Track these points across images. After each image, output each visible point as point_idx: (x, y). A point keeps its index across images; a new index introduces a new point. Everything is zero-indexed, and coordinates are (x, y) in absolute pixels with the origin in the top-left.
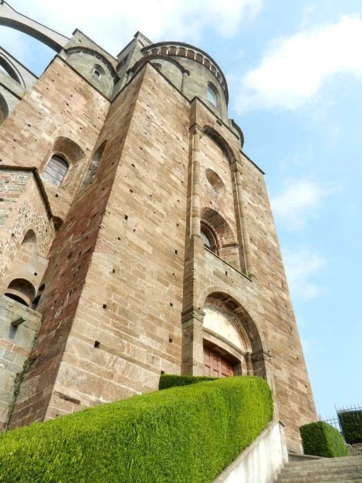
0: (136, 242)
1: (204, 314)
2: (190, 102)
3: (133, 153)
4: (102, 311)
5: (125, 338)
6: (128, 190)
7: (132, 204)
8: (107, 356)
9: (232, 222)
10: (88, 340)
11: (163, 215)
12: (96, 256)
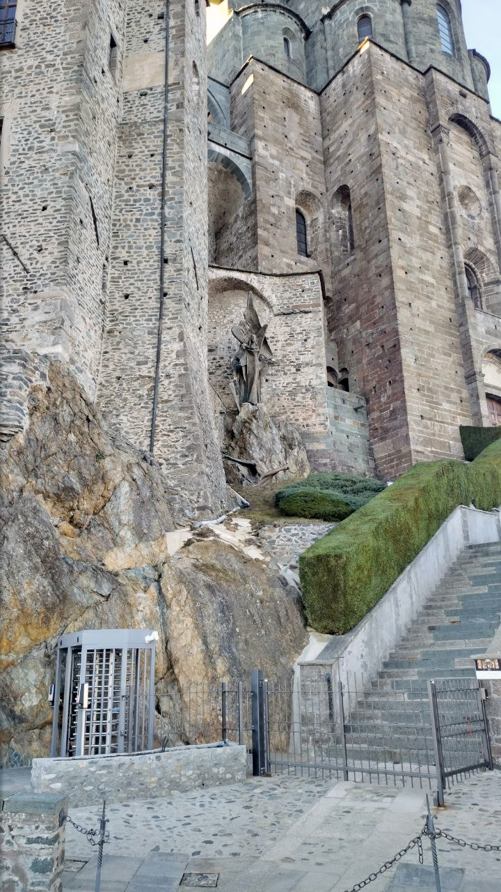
0: (422, 327)
1: (484, 376)
2: (424, 74)
3: (398, 223)
4: (418, 395)
5: (435, 408)
7: (410, 288)
8: (429, 423)
11: (433, 284)
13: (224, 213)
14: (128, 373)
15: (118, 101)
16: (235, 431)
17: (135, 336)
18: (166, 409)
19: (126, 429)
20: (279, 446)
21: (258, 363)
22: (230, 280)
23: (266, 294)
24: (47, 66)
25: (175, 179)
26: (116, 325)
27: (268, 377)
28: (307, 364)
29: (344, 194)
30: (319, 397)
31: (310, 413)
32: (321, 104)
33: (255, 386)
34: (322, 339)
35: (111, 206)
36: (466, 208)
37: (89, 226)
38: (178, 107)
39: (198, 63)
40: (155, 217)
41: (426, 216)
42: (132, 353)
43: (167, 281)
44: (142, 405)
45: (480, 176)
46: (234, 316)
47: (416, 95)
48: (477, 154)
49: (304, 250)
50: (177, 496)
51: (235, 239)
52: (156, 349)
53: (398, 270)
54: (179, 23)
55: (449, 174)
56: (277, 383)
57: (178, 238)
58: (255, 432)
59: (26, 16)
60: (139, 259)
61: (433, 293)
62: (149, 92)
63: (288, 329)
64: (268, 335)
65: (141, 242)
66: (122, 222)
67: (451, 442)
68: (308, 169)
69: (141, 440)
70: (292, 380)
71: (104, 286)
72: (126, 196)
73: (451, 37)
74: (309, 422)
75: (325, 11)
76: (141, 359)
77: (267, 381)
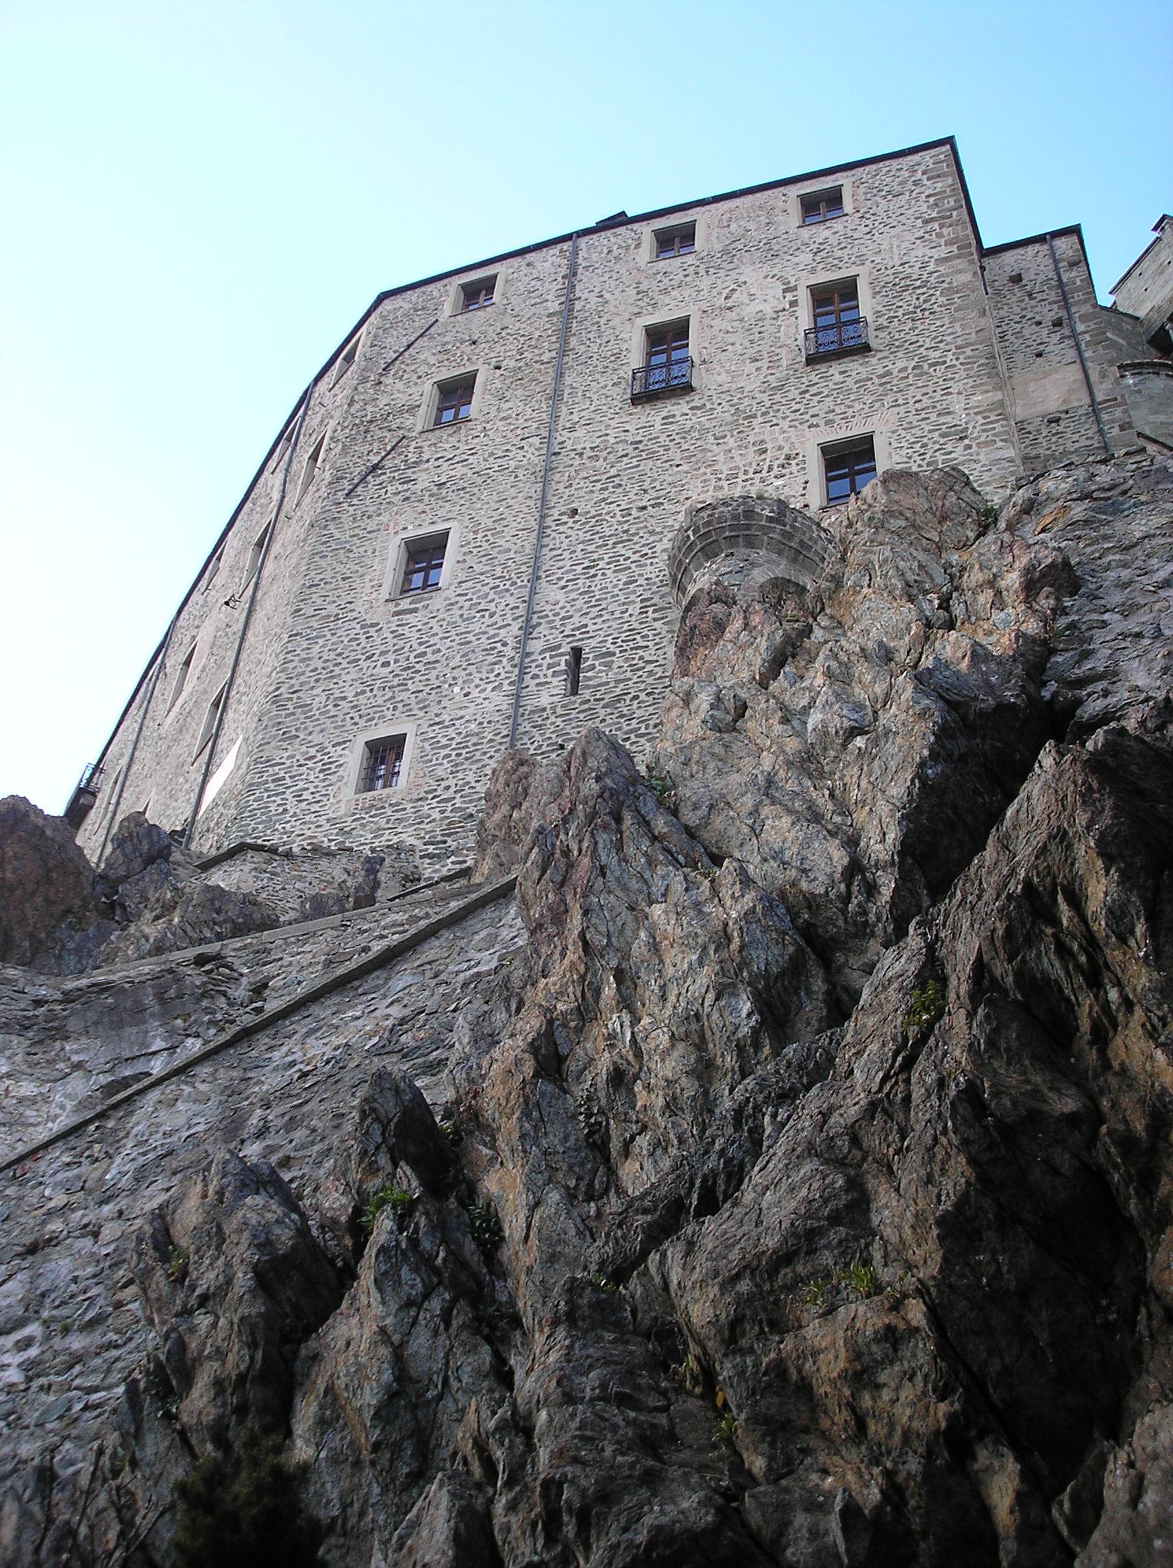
24: (931, 365)
38: (1122, 428)
59: (878, 314)
62: (1063, 416)
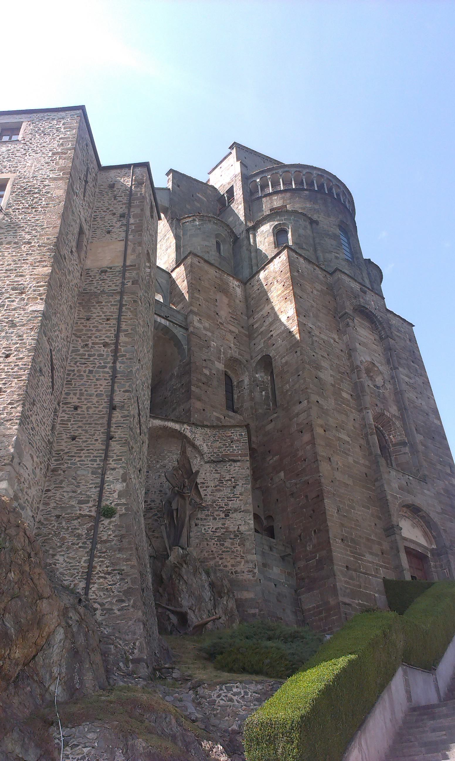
2: (331, 274)
6: (321, 431)
9: (397, 418)
10: (342, 566)
11: (348, 442)
12: (326, 501)
13: (161, 372)
14: (69, 511)
15: (81, 275)
16: (164, 577)
17: (78, 476)
18: (104, 550)
19: (61, 570)
20: (207, 594)
21: (188, 507)
22: (165, 428)
23: (198, 443)
25: (127, 339)
26: (60, 464)
27: (197, 521)
28: (236, 510)
29: (267, 363)
30: (247, 544)
31: (239, 559)
32: (245, 291)
33: (185, 531)
34: (249, 486)
35: (67, 358)
36: (371, 380)
37: (47, 374)
39: (150, 252)
40: (107, 370)
41: (339, 385)
42: (74, 492)
43: (114, 426)
44: (80, 545)
45: (381, 354)
46: (166, 462)
47: (325, 289)
48: (377, 338)
49: (231, 406)
50: (112, 646)
51: (169, 394)
52: (98, 489)
53: (317, 428)
54: (138, 221)
55: (357, 351)
56: (206, 527)
57: (127, 388)
58: (185, 577)
60: (89, 405)
61: (349, 450)
62: (108, 270)
63: (217, 476)
64: (199, 481)
65: (92, 391)
66: (75, 372)
67: (376, 595)
68: (236, 341)
69: (76, 582)
70: (220, 526)
71: (53, 428)
72: (82, 351)
73: (350, 249)
74: (238, 569)
75: (250, 224)
76: (83, 498)
77: (196, 525)
